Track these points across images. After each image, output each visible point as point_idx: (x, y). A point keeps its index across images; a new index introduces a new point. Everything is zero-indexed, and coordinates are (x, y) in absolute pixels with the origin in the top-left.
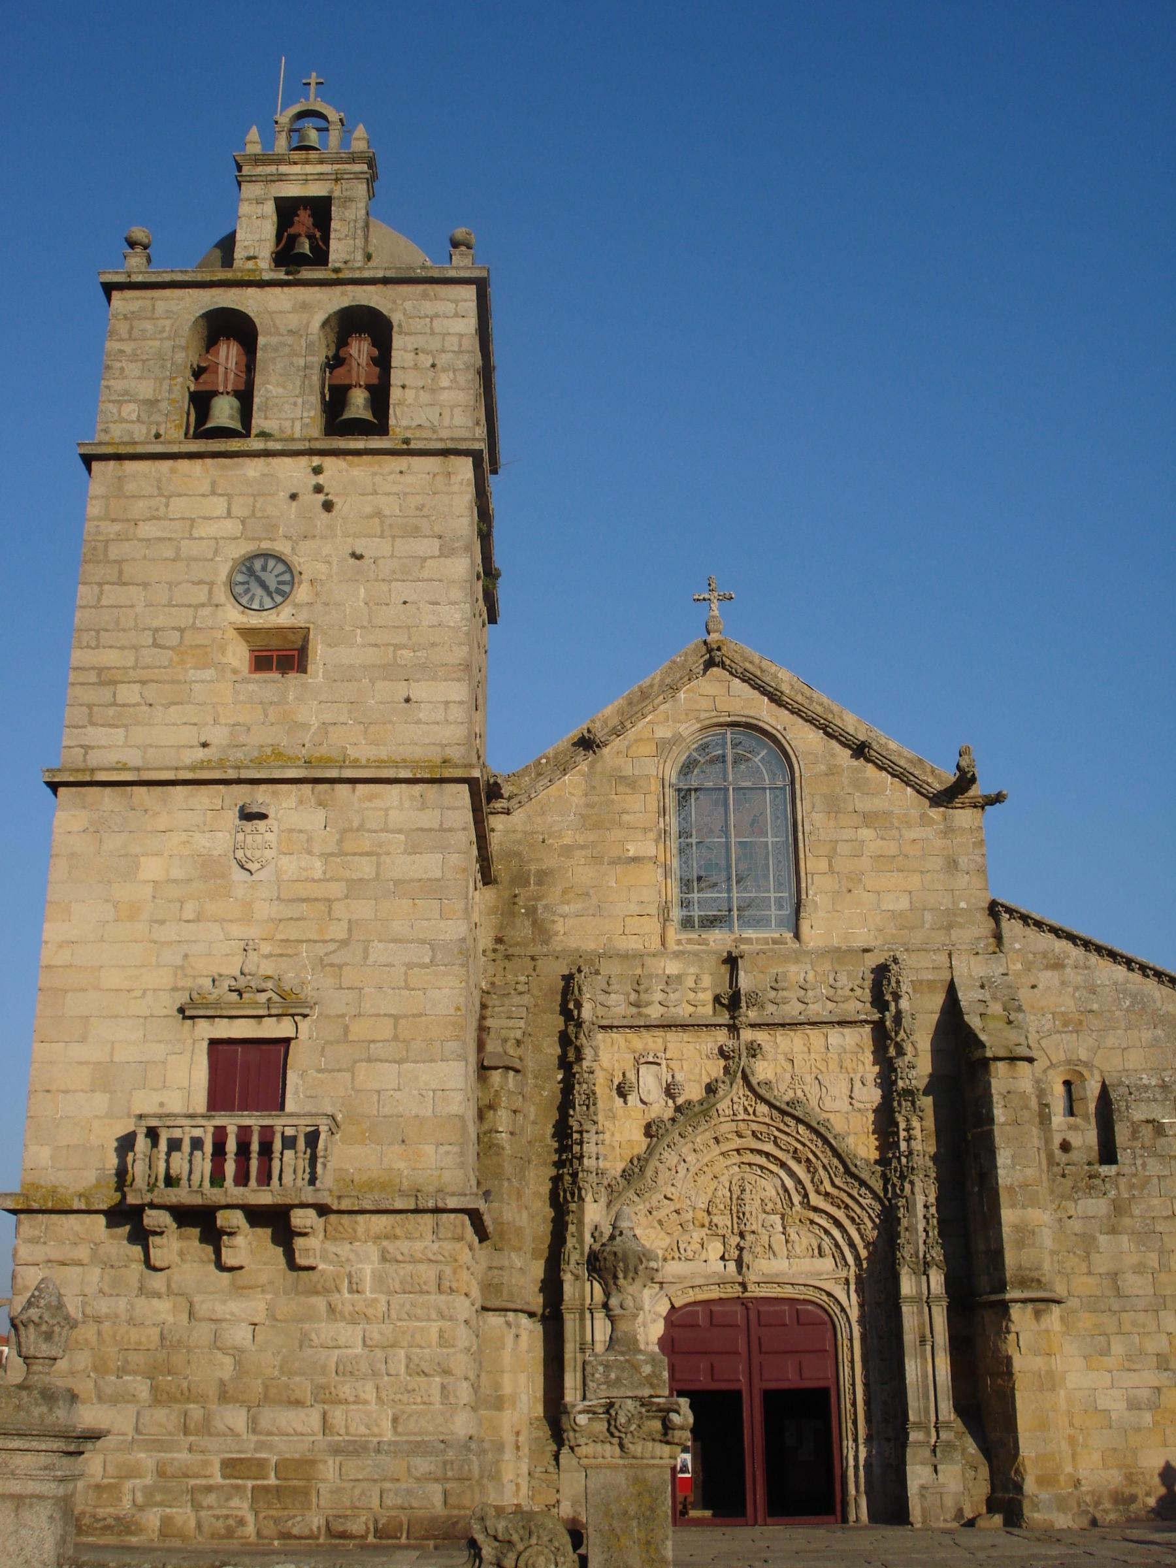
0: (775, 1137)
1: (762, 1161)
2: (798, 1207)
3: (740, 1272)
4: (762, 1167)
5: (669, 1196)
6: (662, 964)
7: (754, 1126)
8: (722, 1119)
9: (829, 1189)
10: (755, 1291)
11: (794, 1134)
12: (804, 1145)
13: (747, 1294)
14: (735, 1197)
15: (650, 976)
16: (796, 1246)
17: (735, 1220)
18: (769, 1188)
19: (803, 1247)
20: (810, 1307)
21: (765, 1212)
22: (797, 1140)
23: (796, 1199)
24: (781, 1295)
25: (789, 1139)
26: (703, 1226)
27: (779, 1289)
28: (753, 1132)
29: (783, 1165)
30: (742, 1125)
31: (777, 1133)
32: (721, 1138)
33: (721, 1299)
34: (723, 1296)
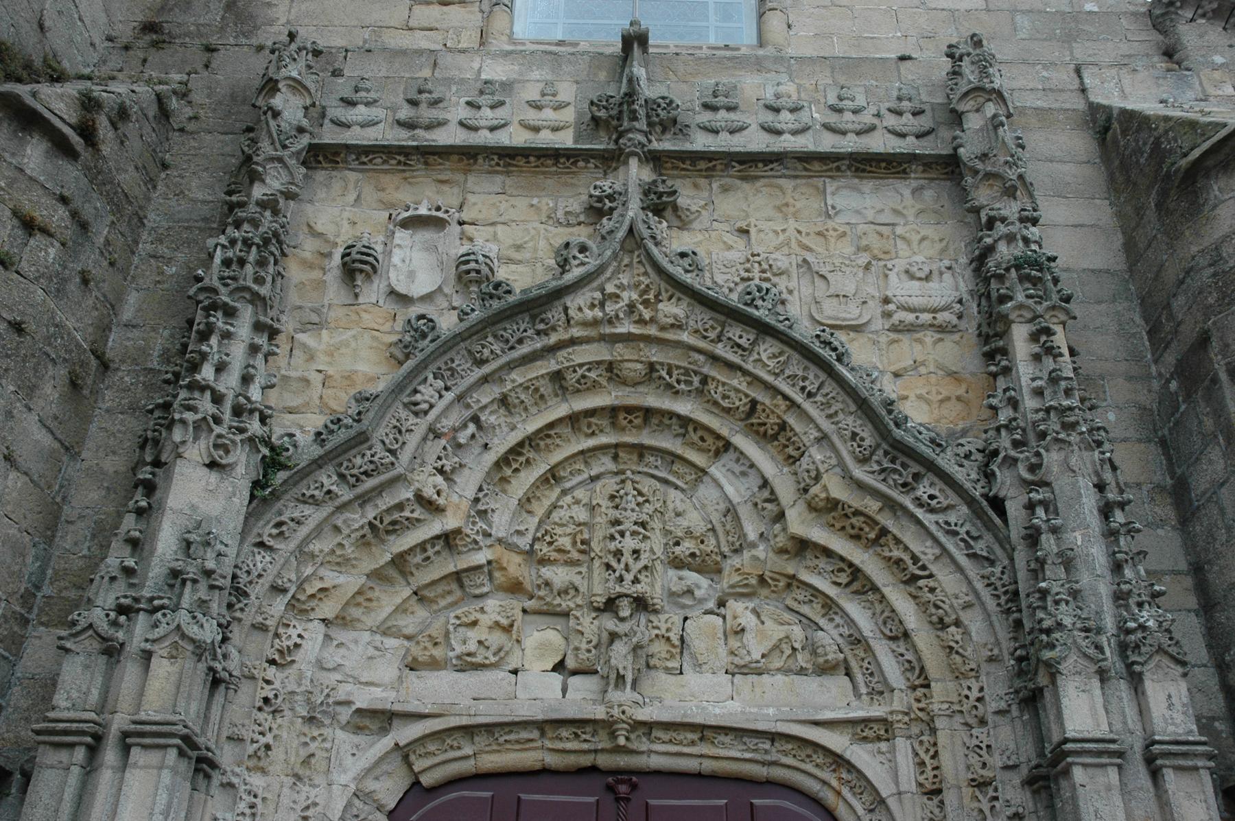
0: (705, 380)
5: (429, 492)
6: (476, 65)
8: (576, 332)
9: (838, 490)
15: (448, 81)
20: (787, 804)
24: (708, 766)
25: (738, 382)
30: (621, 351)
34: (552, 760)
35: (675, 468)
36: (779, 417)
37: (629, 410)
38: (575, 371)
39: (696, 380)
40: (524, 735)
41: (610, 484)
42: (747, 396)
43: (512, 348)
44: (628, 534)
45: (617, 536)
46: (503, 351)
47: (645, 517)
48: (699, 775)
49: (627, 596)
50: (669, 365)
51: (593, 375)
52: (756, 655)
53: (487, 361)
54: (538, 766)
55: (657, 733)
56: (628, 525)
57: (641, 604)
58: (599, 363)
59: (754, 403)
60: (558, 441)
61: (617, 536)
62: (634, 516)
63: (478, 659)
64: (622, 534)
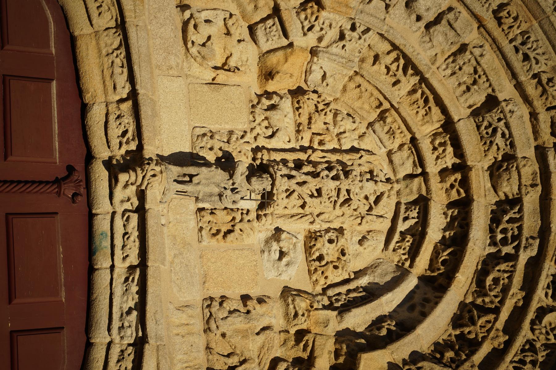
0: (513, 258)
1: (435, 232)
2: (335, 324)
3: (162, 159)
4: (418, 234)
7: (531, 200)
10: (111, 202)
11: (534, 305)
12: (512, 328)
13: (101, 175)
14: (345, 158)
16: (237, 323)
17: (290, 157)
18: (367, 252)
19: (237, 340)
21: (312, 237)
22: (518, 314)
23: (359, 319)
24: (102, 279)
26: (268, 75)
27: (121, 267)
28: (516, 202)
29: (435, 285)
30: (530, 170)
31: (523, 258)
32: (492, 116)
33: (84, 109)
34: (96, 115)
35: (409, 238)
36: (484, 338)
37: (465, 183)
38: (499, 120)
39: (508, 249)
40: (122, 79)
41: (383, 169)
42: (502, 302)
43: (517, 50)
44: (338, 183)
45: (334, 173)
46: (511, 41)
47: (354, 204)
48: (91, 270)
49: (273, 185)
50: (521, 219)
51: (499, 139)
52: (225, 327)
53: (500, 24)
54: (88, 98)
55: (134, 218)
56: (345, 185)
57: (266, 200)
58: (512, 145)
59: (497, 311)
60: (422, 112)
61: (334, 173)
62: (355, 189)
63: (192, 35)
64: (336, 178)
